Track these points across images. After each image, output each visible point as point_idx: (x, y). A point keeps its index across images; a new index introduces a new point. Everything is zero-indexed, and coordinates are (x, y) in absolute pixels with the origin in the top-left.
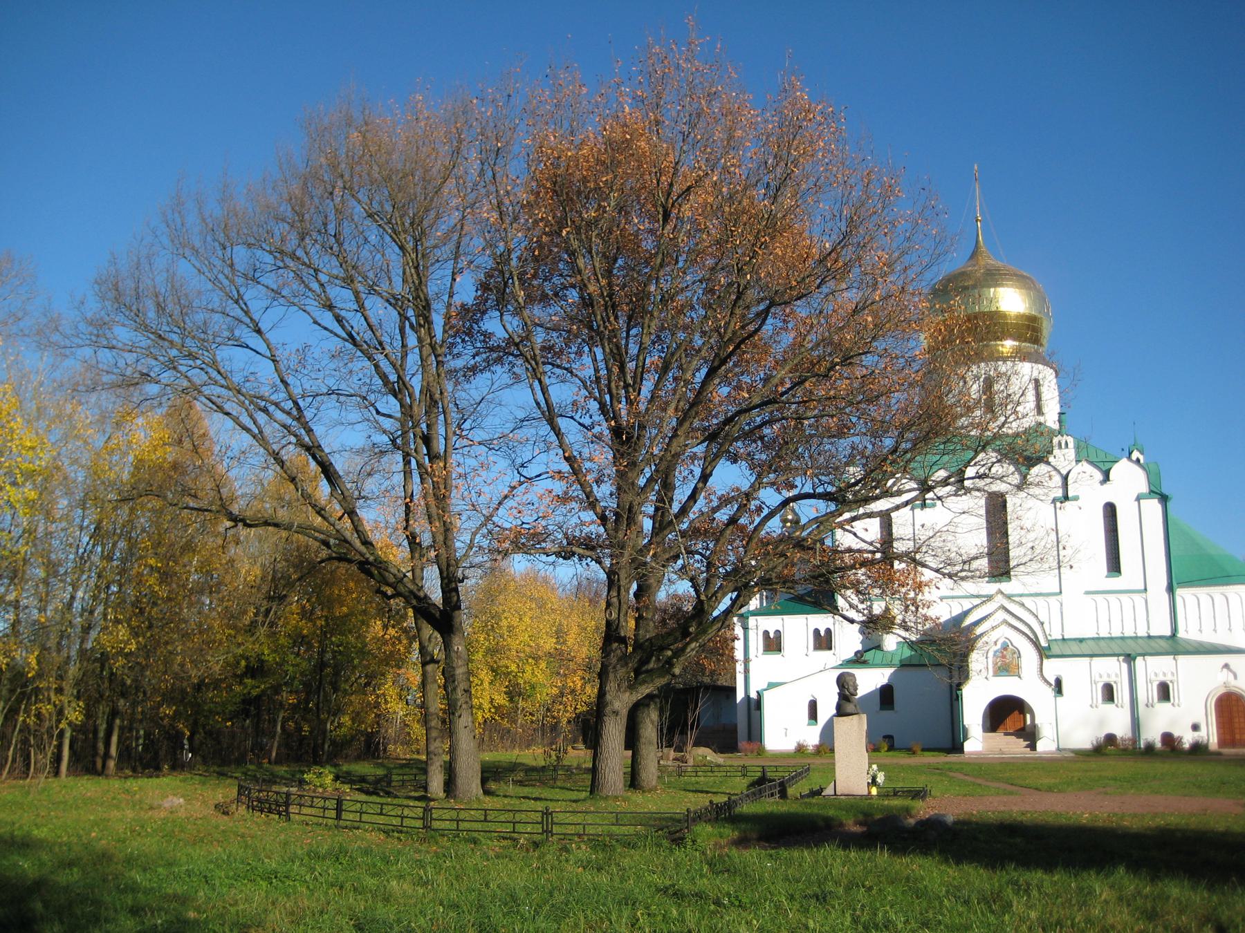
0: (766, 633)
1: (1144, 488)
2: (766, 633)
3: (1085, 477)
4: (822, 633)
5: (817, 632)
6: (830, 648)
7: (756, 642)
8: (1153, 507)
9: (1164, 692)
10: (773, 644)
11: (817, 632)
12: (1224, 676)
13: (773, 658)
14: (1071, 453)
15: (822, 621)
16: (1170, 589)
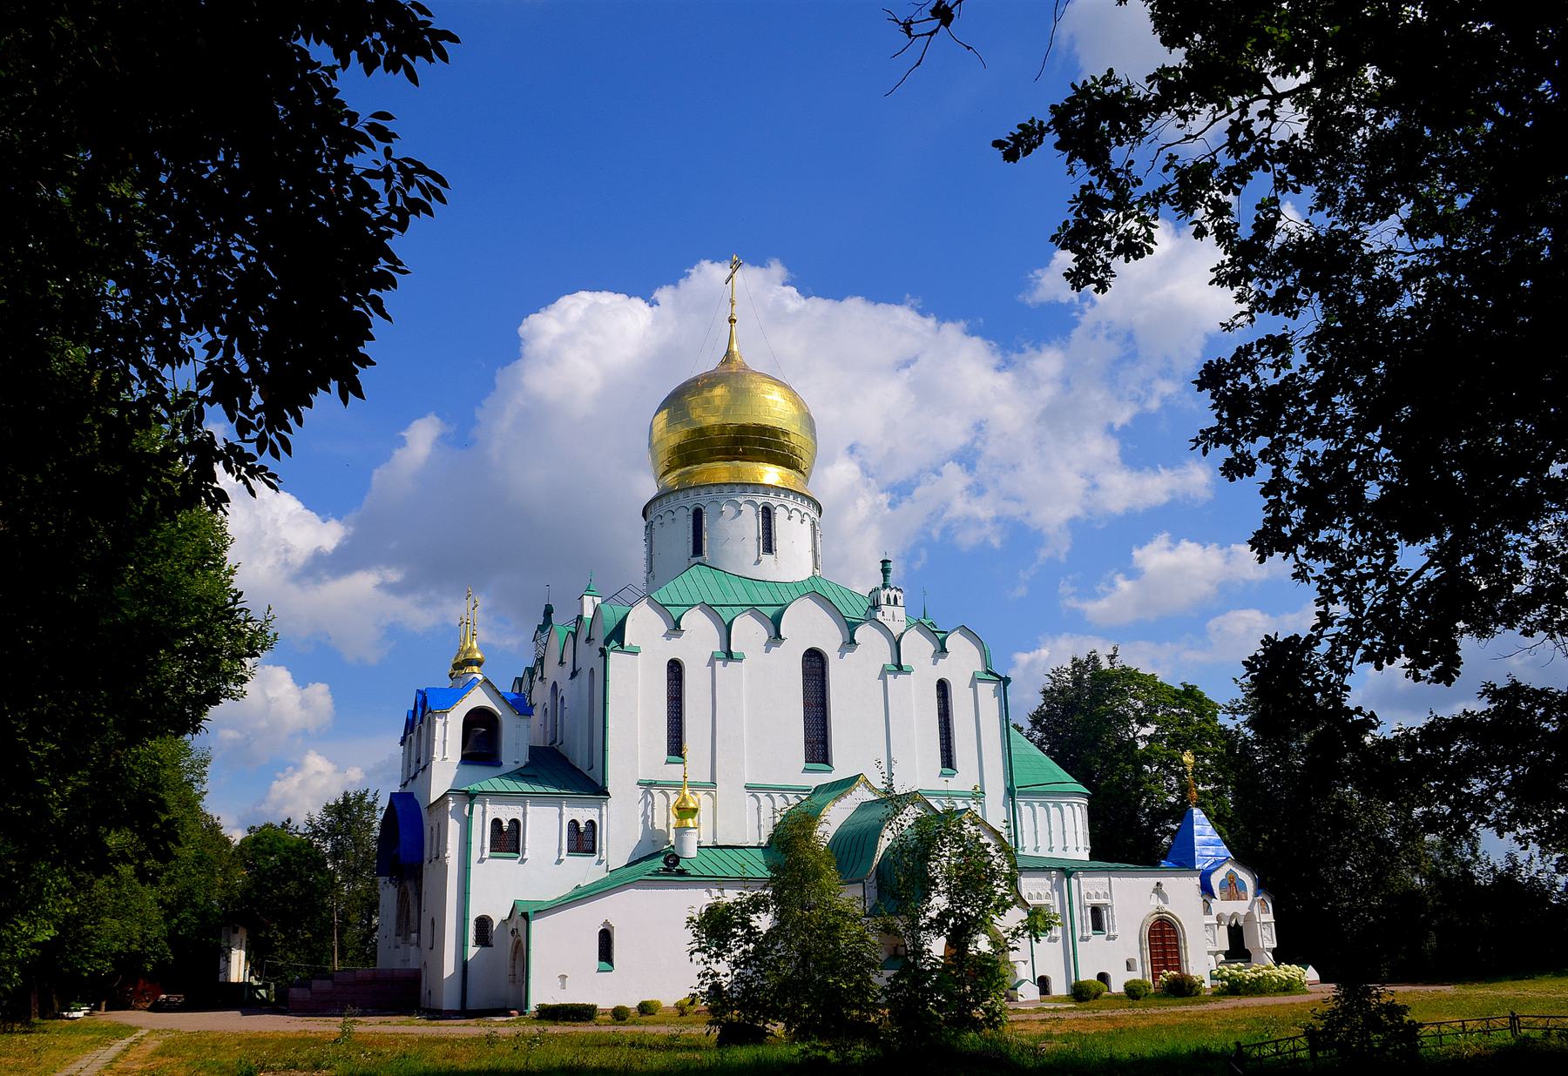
0: (497, 823)
1: (978, 667)
2: (497, 823)
3: (917, 647)
5: (574, 824)
6: (593, 851)
7: (481, 836)
8: (987, 690)
9: (1097, 917)
10: (507, 840)
11: (574, 824)
12: (1155, 902)
13: (505, 866)
14: (900, 612)
15: (583, 815)
16: (1010, 793)
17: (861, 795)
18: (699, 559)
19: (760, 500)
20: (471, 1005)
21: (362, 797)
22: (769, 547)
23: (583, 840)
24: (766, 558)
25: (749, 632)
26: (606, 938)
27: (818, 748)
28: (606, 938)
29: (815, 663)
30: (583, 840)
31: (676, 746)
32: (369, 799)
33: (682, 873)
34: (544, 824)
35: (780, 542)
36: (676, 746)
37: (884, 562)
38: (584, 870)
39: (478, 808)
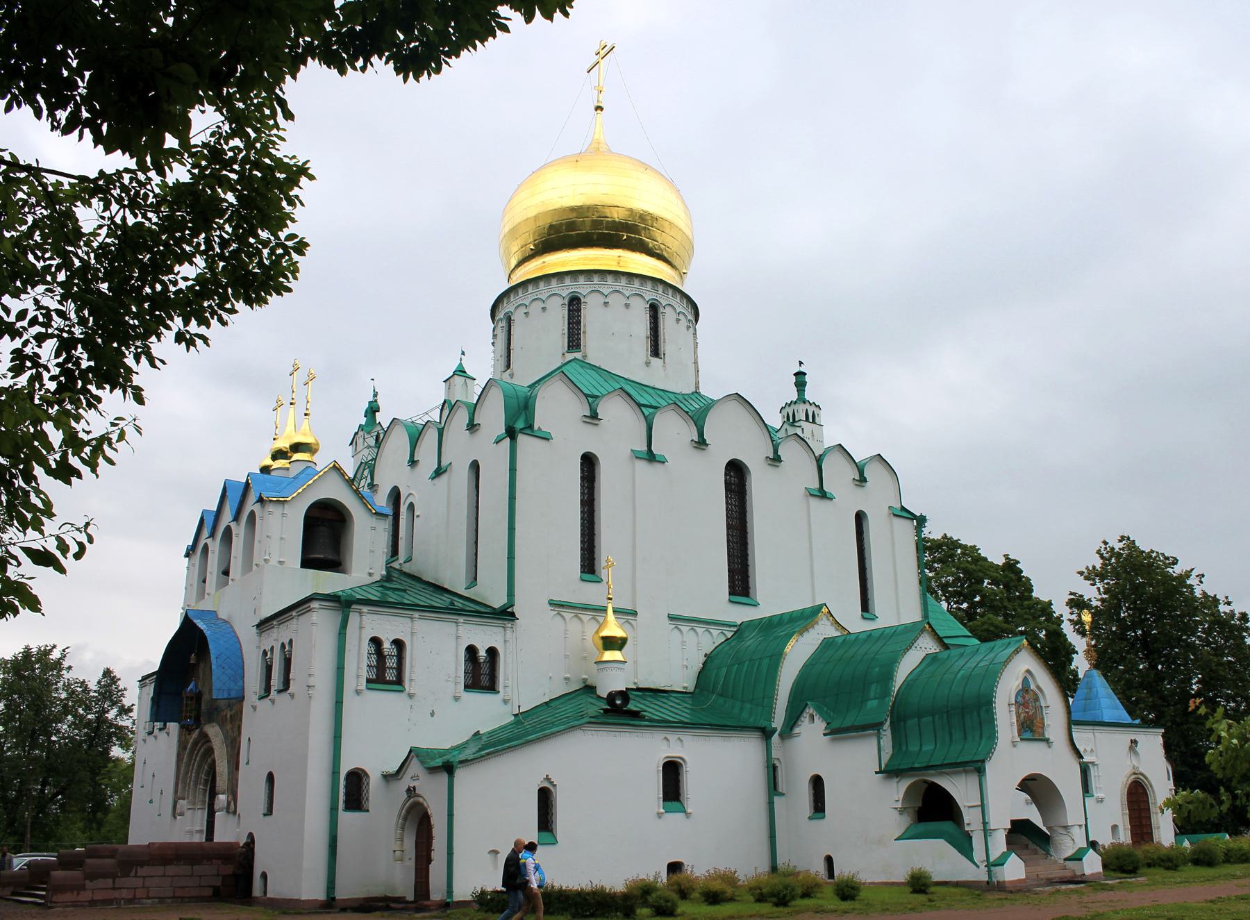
4: (482, 654)
5: (471, 651)
7: (359, 663)
10: (388, 669)
11: (471, 651)
15: (483, 636)
17: (823, 630)
18: (578, 355)
19: (649, 296)
20: (341, 894)
21: (46, 653)
22: (655, 351)
23: (481, 673)
24: (654, 360)
25: (672, 432)
26: (545, 798)
27: (740, 582)
28: (545, 798)
29: (736, 473)
30: (481, 673)
31: (589, 564)
32: (55, 655)
33: (635, 715)
34: (437, 648)
35: (667, 346)
36: (589, 564)
37: (799, 375)
38: (487, 713)
39: (354, 619)
